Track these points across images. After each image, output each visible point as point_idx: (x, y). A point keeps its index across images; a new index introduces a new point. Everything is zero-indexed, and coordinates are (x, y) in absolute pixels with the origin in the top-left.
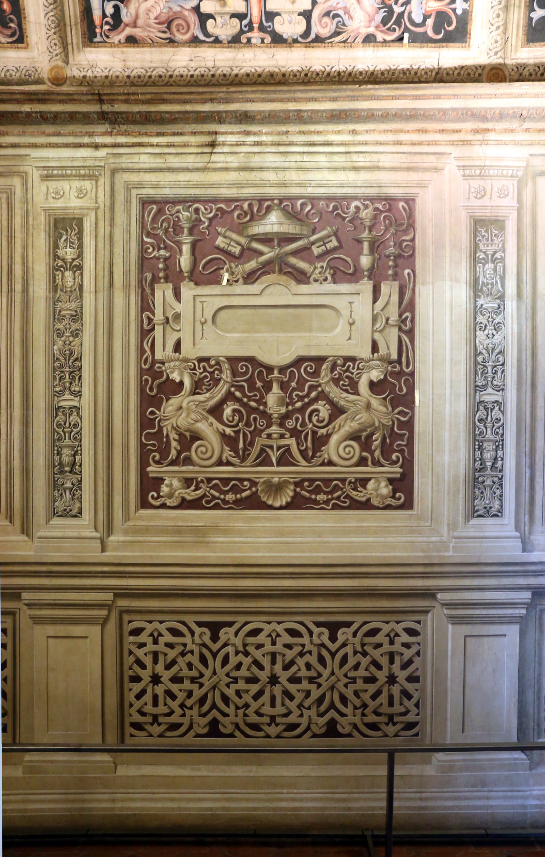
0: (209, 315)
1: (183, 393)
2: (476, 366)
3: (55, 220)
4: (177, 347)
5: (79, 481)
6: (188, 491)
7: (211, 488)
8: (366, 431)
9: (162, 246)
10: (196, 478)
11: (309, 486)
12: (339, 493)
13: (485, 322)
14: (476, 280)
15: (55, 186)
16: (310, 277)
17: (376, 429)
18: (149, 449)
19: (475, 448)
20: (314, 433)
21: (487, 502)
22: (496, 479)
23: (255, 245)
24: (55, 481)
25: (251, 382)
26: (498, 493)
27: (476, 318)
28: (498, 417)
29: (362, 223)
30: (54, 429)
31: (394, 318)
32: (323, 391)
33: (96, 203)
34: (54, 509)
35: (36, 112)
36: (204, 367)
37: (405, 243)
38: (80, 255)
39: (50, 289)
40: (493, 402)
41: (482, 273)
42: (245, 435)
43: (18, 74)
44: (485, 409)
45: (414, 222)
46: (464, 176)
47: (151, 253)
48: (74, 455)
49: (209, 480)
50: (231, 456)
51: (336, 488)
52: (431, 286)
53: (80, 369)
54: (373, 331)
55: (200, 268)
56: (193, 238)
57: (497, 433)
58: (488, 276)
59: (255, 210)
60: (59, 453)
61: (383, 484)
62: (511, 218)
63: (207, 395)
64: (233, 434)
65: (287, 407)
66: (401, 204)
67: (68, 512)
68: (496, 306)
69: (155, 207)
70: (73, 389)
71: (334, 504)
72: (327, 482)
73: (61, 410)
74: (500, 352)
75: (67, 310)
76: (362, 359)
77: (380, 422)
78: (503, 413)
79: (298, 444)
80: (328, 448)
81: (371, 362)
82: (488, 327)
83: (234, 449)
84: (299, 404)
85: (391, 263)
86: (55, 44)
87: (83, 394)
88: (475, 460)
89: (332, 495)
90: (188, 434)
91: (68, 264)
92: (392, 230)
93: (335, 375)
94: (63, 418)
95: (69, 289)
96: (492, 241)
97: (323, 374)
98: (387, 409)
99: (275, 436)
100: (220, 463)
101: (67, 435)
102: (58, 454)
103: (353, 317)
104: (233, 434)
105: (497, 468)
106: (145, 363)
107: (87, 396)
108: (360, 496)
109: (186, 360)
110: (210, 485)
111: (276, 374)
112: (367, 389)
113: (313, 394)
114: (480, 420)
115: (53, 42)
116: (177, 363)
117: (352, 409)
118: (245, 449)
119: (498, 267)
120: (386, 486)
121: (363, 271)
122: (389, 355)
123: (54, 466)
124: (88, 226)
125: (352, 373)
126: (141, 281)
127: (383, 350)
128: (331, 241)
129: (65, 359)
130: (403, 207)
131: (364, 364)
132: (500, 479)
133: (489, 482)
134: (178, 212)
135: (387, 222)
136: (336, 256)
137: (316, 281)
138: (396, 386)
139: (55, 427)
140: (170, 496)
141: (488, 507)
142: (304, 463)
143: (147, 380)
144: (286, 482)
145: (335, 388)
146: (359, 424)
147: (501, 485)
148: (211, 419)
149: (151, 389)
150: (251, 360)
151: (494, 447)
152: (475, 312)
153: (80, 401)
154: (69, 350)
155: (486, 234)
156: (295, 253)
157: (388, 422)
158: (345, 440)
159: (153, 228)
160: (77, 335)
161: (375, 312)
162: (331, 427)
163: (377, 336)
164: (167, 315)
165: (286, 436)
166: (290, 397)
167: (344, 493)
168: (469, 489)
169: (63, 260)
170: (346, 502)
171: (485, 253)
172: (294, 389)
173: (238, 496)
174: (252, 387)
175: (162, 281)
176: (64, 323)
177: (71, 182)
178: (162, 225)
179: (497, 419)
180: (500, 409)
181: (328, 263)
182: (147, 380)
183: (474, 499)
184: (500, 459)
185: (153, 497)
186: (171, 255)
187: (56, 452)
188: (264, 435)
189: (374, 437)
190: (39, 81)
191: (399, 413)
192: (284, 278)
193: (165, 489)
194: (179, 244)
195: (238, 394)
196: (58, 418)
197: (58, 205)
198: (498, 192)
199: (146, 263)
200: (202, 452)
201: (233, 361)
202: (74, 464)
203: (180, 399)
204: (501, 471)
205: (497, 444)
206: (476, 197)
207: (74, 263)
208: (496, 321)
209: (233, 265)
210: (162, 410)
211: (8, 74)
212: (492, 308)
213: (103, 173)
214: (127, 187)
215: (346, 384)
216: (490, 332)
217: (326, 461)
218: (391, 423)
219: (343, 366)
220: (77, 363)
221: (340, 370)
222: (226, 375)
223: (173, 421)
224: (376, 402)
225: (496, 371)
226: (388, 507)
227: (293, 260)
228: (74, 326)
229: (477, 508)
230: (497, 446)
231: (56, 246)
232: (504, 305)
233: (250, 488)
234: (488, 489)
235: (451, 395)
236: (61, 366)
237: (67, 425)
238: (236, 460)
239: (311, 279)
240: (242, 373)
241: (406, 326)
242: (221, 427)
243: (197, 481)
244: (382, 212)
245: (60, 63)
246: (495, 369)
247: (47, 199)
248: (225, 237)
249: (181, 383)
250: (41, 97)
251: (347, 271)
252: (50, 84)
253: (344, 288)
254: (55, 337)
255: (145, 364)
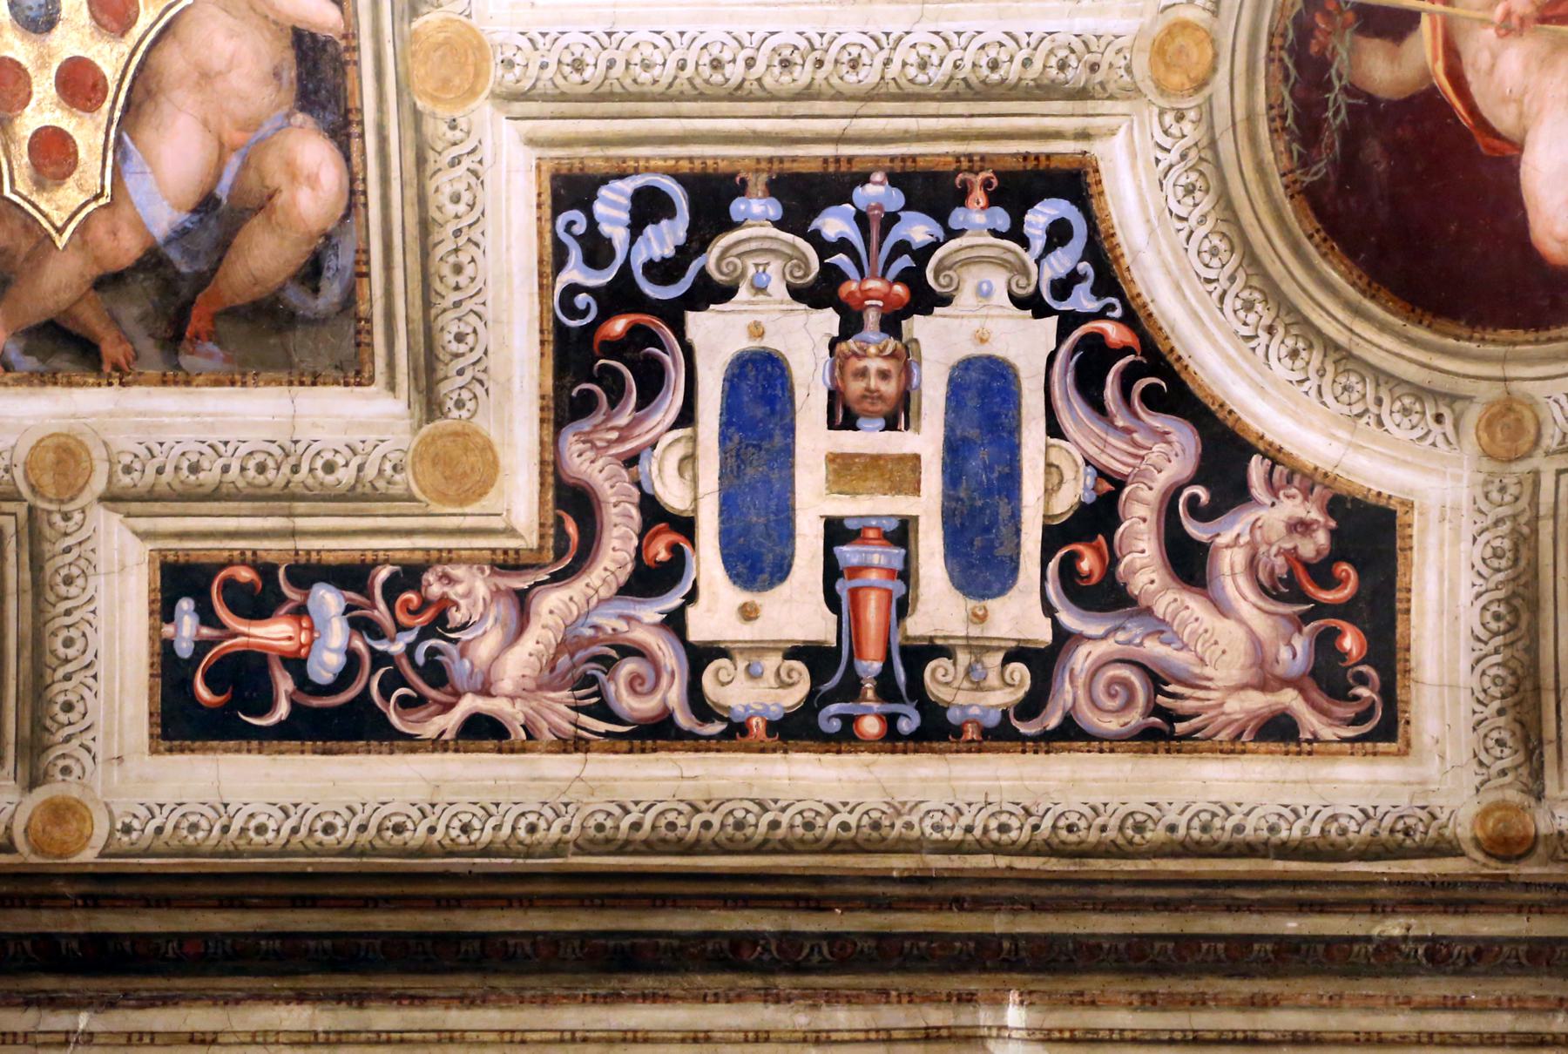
35: (1419, 940)
43: (1368, 829)
86: (1500, 743)
115: (1495, 735)
190: (1444, 848)
211: (1333, 828)
245: (1513, 796)
250: (1462, 893)
252: (1479, 856)
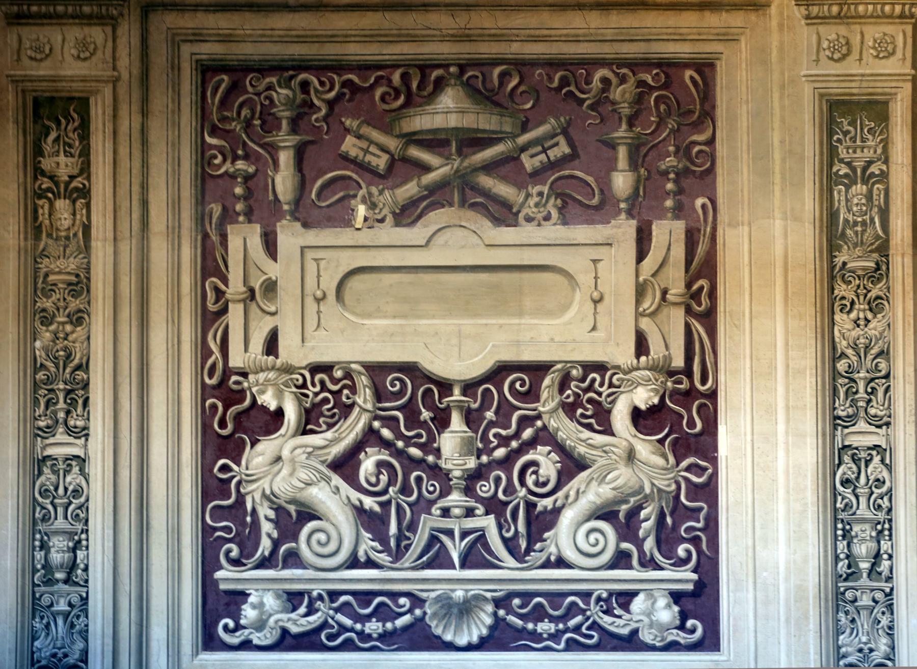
0: (330, 284)
1: (282, 431)
2: (834, 379)
3: (36, 101)
4: (272, 345)
5: (82, 598)
6: (293, 616)
7: (337, 610)
8: (626, 502)
9: (240, 152)
10: (309, 592)
11: (521, 607)
12: (579, 619)
13: (851, 295)
14: (832, 215)
15: (34, 36)
16: (519, 212)
17: (647, 498)
18: (219, 537)
19: (836, 536)
20: (531, 506)
21: (864, 639)
22: (879, 596)
23: (415, 152)
24: (35, 600)
25: (410, 410)
26: (885, 621)
27: (833, 289)
28: (880, 477)
29: (614, 111)
30: (34, 499)
31: (677, 289)
32: (545, 427)
33: (114, 69)
34: (33, 653)
36: (322, 383)
37: (697, 149)
38: (85, 169)
39: (26, 233)
40: (869, 448)
41: (843, 203)
42: (400, 510)
44: (854, 460)
45: (714, 107)
46: (808, 17)
47: (219, 167)
48: (74, 550)
49: (333, 595)
50: (373, 548)
51: (573, 610)
52: (746, 228)
53: (86, 386)
54: (638, 315)
55: (313, 196)
56: (298, 137)
57: (880, 506)
58: (855, 209)
59: (414, 85)
60: (44, 546)
61: (662, 602)
62: (899, 97)
63: (329, 435)
64: (377, 508)
65: (478, 457)
66: (689, 73)
67: (60, 660)
68: (873, 265)
69: (225, 77)
70: (72, 423)
71: (568, 641)
72: (555, 597)
73: (49, 463)
74: (880, 354)
75: (59, 273)
76: (618, 367)
77: (653, 484)
78: (889, 468)
79: (500, 527)
80: (556, 535)
81: (635, 373)
82: (857, 306)
83: (381, 537)
84: (500, 453)
85: (670, 186)
87: (92, 431)
88: (837, 559)
89: (565, 624)
90: (292, 509)
91: (62, 186)
92: (672, 124)
93: (568, 397)
94: (53, 478)
95: (63, 234)
96: (862, 141)
97: (544, 395)
98: (667, 460)
99: (456, 511)
100: (353, 563)
101: (60, 510)
102: (42, 547)
103: (599, 288)
104: (377, 508)
105: (880, 574)
106: (211, 375)
107: (100, 437)
108: (619, 625)
109: (288, 369)
110: (335, 605)
111: (457, 395)
112: (628, 422)
113: (527, 433)
114: (846, 482)
116: (272, 375)
117: (601, 462)
118: (400, 537)
119: (875, 192)
120: (668, 606)
121: (619, 201)
122: (668, 359)
123: (35, 571)
124: (99, 112)
125: (600, 394)
126: (201, 219)
127: (656, 350)
128: (557, 144)
129: (57, 368)
130: (692, 78)
131: (621, 376)
132: (886, 595)
133: (865, 600)
134: (270, 87)
135: (662, 107)
136: (567, 172)
137: (529, 219)
138: (682, 417)
139: (37, 495)
140: (260, 625)
141: (866, 648)
142: (511, 562)
143: (214, 407)
144: (478, 598)
145: (567, 421)
146: (614, 489)
147: (890, 607)
148: (337, 480)
149: (223, 424)
150: (411, 369)
151: (874, 534)
152: (832, 278)
153: (86, 446)
154: (65, 349)
155: (851, 129)
156: (489, 168)
157: (669, 486)
158: (588, 520)
159: (224, 119)
160: (79, 322)
161: (641, 279)
162: (560, 494)
163: (646, 324)
164: (252, 284)
165: (478, 512)
166: (485, 438)
167: (588, 618)
168: (827, 613)
169: (52, 178)
170: (591, 637)
171: (849, 164)
172: (491, 424)
173: (389, 625)
174: (413, 419)
175: (241, 218)
176: (54, 297)
177: (64, 28)
178: (239, 113)
179: (878, 480)
180: (882, 461)
181: (551, 188)
182: (214, 407)
183: (838, 632)
184: (885, 556)
185: (226, 628)
186: (257, 170)
187: (37, 543)
188: (436, 511)
189: (643, 514)
191: (687, 469)
192: (470, 214)
193: (249, 613)
194: (272, 149)
195: (386, 433)
196: (42, 479)
197: (41, 73)
198: (874, 48)
199: (210, 184)
200: (319, 543)
201: (376, 370)
202: (73, 566)
203: (277, 442)
204: (889, 579)
205: (879, 527)
206: (831, 59)
207: (74, 184)
208: (873, 294)
209: (374, 190)
210: (243, 462)
212: (864, 268)
213: (126, 11)
214: (173, 42)
215: (589, 413)
216: (861, 315)
217: (553, 558)
218: (674, 487)
219: (583, 380)
220: (81, 375)
221: (577, 387)
222: (364, 398)
223: (265, 484)
224: (644, 448)
225: (873, 388)
226: (672, 647)
227: (486, 181)
228: (75, 304)
229: (843, 650)
230: (880, 532)
231: (38, 152)
232: (888, 264)
233: (410, 611)
234: (864, 613)
235: (787, 433)
236: (49, 381)
237: (61, 491)
238: (383, 558)
239: (521, 216)
240: (392, 393)
241: (700, 305)
242: (355, 495)
243: (309, 597)
244: (652, 88)
246: (872, 384)
247: (19, 60)
248: (359, 137)
249: (279, 414)
251: (587, 202)
253: (582, 233)
254: (37, 323)
255: (211, 376)
